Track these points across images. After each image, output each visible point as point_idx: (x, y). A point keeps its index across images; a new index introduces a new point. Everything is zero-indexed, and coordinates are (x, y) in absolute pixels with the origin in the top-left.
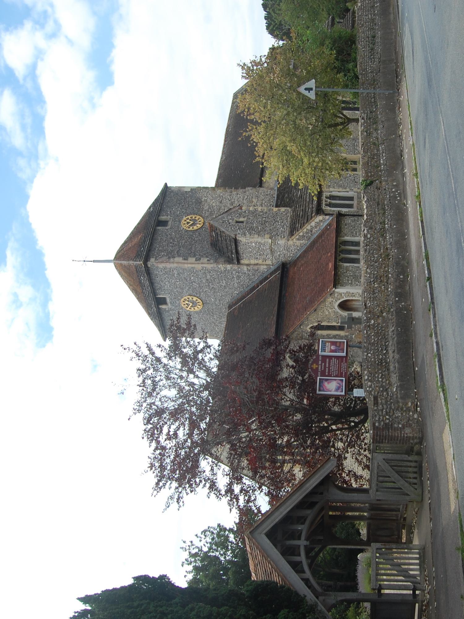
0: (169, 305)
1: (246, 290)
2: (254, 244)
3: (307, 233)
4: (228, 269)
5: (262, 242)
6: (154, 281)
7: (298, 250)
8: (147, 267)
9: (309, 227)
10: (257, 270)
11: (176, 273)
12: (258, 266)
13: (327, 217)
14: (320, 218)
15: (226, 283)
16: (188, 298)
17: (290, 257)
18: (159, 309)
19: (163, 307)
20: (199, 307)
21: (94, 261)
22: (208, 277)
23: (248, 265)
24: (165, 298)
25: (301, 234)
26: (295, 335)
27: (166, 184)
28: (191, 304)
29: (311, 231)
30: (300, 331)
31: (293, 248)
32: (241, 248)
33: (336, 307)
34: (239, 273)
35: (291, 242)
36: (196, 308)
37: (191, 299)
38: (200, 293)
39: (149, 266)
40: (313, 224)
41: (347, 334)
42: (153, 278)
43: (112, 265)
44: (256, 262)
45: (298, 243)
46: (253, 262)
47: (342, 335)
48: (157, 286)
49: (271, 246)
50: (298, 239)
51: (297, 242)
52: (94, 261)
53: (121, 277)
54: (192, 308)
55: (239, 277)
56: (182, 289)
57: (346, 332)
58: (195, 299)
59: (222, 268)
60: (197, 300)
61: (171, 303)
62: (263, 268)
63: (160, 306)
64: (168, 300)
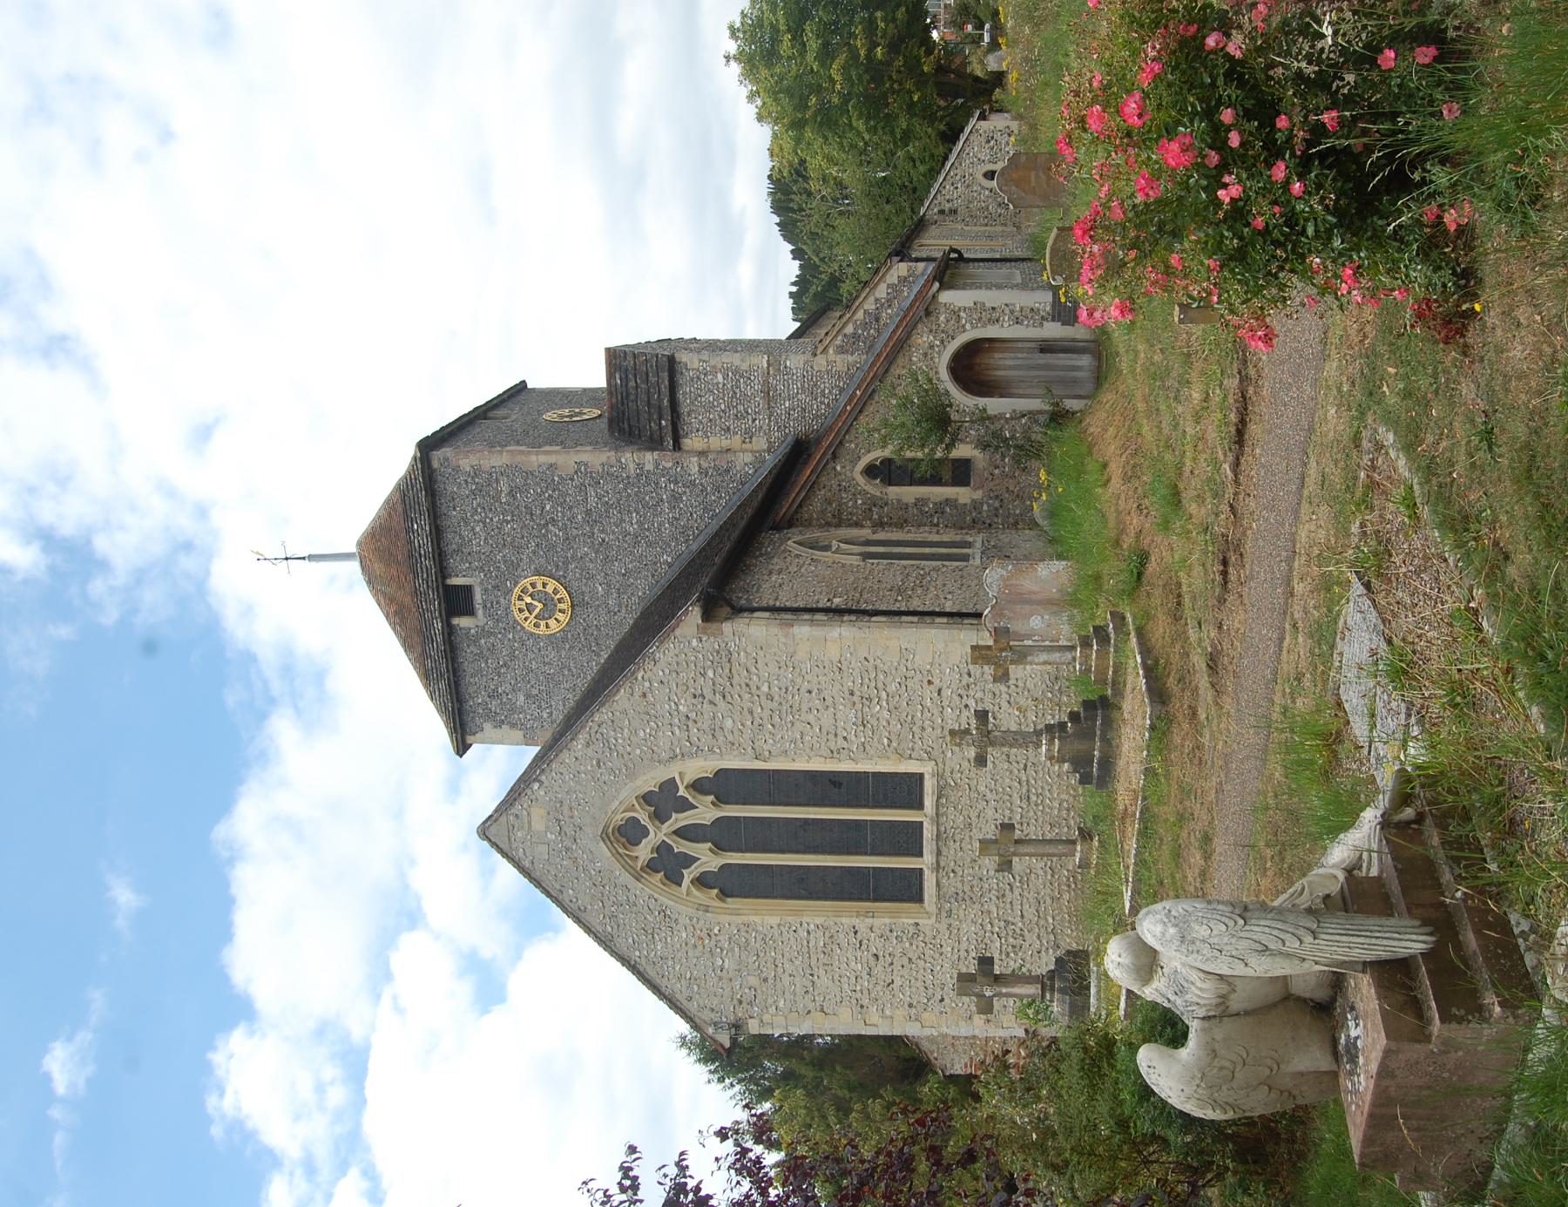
0: (480, 612)
1: (695, 547)
2: (720, 376)
3: (865, 325)
4: (649, 467)
5: (744, 366)
6: (444, 523)
7: (841, 390)
8: (430, 466)
9: (870, 305)
10: (727, 471)
11: (505, 489)
12: (730, 456)
13: (921, 265)
14: (901, 269)
15: (640, 524)
16: (533, 585)
17: (816, 417)
18: (450, 631)
19: (462, 622)
20: (560, 616)
21: (311, 558)
22: (592, 501)
23: (702, 454)
24: (468, 590)
25: (849, 329)
26: (816, 505)
27: (524, 382)
28: (540, 606)
29: (877, 320)
30: (834, 483)
31: (825, 385)
32: (685, 393)
33: (944, 374)
34: (676, 483)
35: (820, 362)
36: (552, 622)
37: (540, 587)
38: (566, 563)
39: (435, 464)
40: (882, 291)
41: (978, 495)
42: (444, 509)
43: (354, 567)
44: (725, 443)
45: (841, 362)
46: (717, 442)
47: (962, 501)
48: (452, 541)
49: (766, 383)
50: (841, 350)
51: (839, 358)
52: (311, 558)
53: (369, 582)
54: (543, 623)
55: (676, 498)
56: (518, 549)
57: (975, 489)
58: (552, 585)
59: (632, 466)
60: (556, 592)
61: (485, 607)
62: (743, 461)
63: (455, 621)
64: (478, 597)
